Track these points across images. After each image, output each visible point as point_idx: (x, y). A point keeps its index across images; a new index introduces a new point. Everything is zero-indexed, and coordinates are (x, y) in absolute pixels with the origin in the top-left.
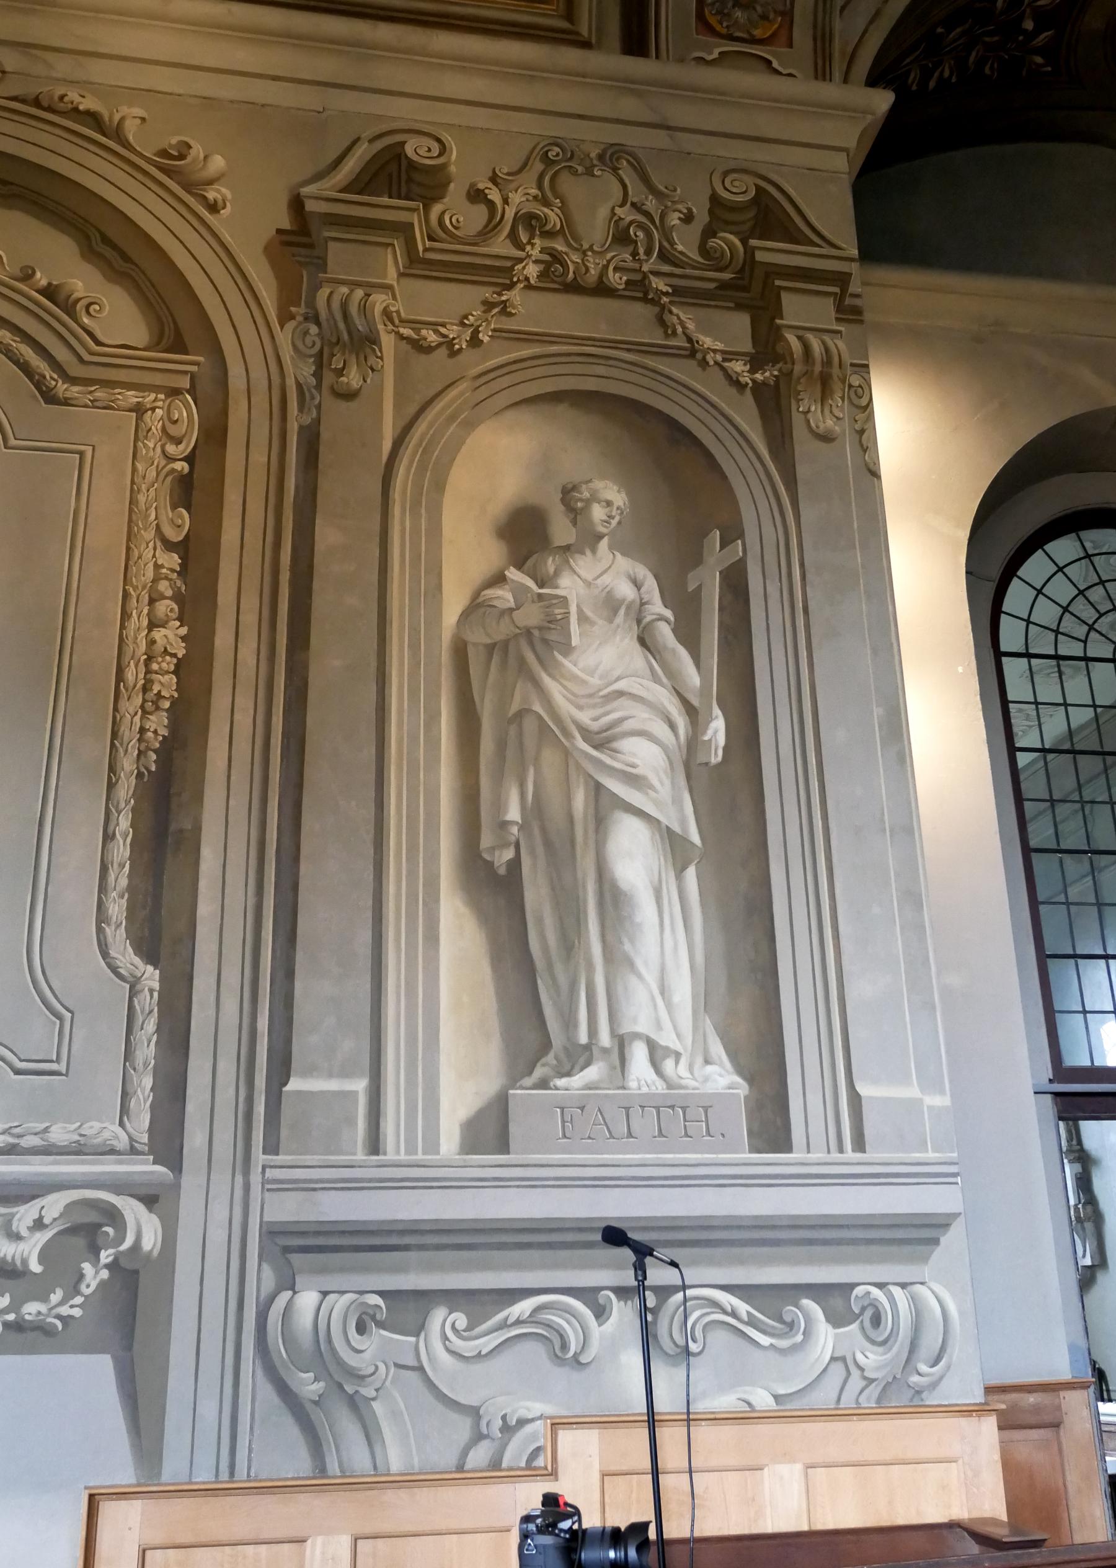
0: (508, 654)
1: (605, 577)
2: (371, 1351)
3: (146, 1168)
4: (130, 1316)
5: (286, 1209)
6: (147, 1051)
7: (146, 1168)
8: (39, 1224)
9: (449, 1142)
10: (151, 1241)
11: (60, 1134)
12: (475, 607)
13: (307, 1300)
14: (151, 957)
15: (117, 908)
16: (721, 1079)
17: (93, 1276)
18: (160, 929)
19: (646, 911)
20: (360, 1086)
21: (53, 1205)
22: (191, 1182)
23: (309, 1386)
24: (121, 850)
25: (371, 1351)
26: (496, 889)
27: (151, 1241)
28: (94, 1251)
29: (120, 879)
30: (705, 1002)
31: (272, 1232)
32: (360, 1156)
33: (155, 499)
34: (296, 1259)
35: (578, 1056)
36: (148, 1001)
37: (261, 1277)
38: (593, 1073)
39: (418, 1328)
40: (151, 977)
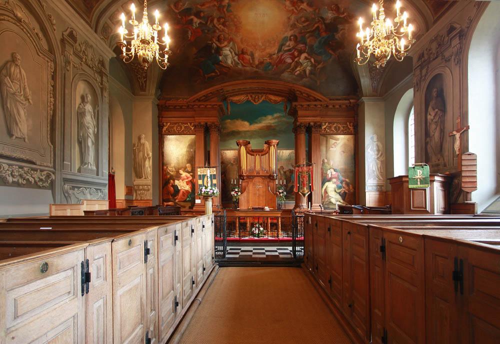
0: (81, 114)
1: (89, 107)
2: (71, 192)
3: (52, 169)
4: (52, 186)
5: (65, 176)
6: (52, 156)
7: (52, 169)
8: (44, 175)
9: (76, 172)
10: (54, 178)
11: (45, 164)
12: (79, 107)
13: (66, 186)
14: (52, 144)
15: (49, 137)
16: (95, 168)
17: (49, 182)
18: (53, 141)
19: (90, 149)
20: (70, 163)
21: (45, 173)
22: (57, 172)
23: (66, 195)
24: (49, 129)
25: (71, 192)
26: (80, 143)
27: (54, 178)
28: (49, 178)
29: (49, 133)
30: (94, 159)
31: (64, 179)
32: (69, 171)
33: (50, 79)
34: (66, 182)
35: (86, 164)
36: (52, 149)
37: (63, 183)
38: (86, 166)
39: (74, 190)
40: (52, 146)
